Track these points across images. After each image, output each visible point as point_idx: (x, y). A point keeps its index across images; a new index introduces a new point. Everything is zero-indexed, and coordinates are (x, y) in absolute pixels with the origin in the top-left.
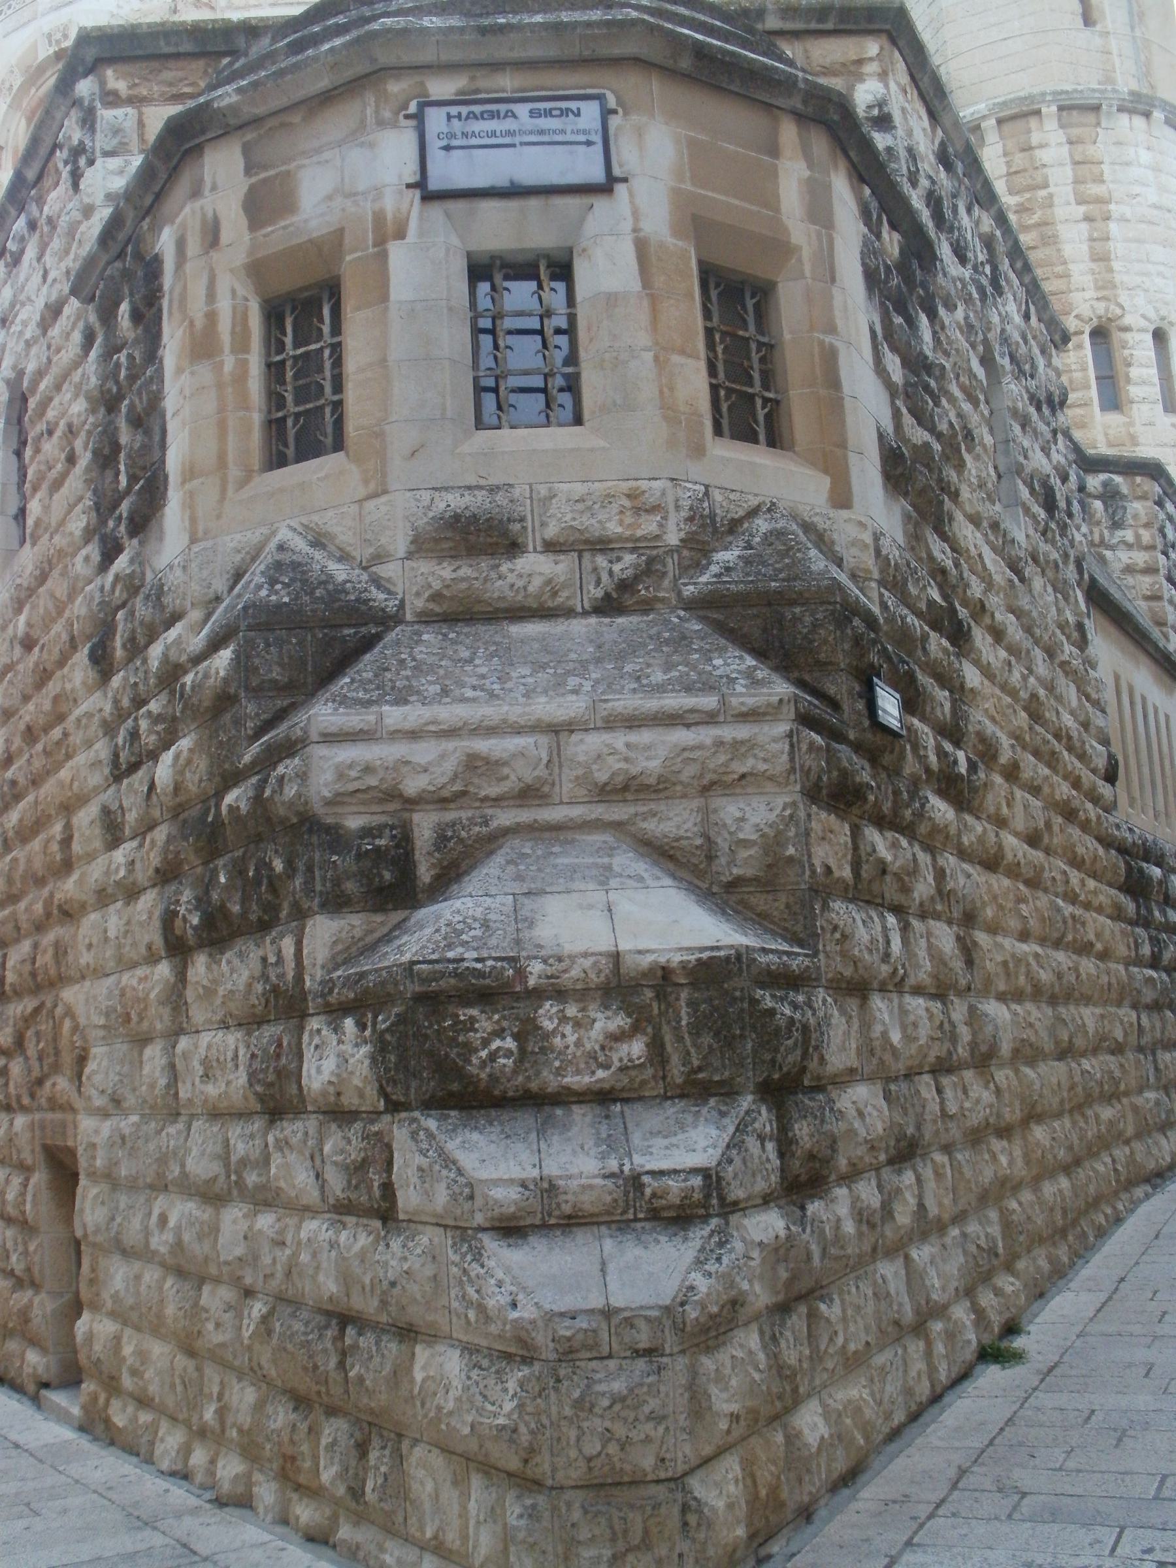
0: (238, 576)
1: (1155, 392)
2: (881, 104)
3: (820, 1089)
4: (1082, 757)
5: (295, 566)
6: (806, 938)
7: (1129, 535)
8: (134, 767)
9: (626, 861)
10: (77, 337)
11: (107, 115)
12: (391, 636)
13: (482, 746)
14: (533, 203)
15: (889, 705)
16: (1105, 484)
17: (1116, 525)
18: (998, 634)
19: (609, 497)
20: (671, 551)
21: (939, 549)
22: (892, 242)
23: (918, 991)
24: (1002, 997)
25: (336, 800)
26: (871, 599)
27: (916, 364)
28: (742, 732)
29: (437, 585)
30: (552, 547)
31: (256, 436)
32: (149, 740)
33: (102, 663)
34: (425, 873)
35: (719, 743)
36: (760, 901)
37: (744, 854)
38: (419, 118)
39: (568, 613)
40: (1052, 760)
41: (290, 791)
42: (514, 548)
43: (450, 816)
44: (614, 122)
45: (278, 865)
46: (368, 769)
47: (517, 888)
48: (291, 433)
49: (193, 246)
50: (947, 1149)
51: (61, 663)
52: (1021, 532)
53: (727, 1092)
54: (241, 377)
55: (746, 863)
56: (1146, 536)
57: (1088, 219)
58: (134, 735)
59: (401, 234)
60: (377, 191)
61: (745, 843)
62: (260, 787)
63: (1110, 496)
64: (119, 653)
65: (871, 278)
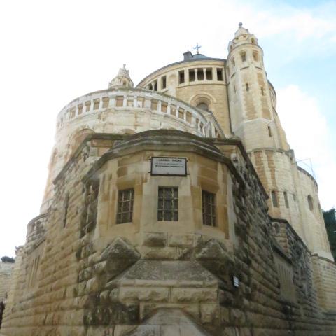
0: (108, 245)
1: (284, 204)
2: (236, 158)
4: (273, 283)
5: (120, 245)
7: (280, 234)
8: (82, 281)
9: (183, 318)
10: (81, 190)
11: (92, 149)
12: (138, 262)
13: (156, 290)
14: (172, 177)
15: (236, 281)
16: (276, 224)
17: (278, 232)
18: (256, 261)
19: (182, 237)
20: (193, 248)
21: (245, 246)
22: (238, 185)
25: (125, 299)
26: (233, 258)
27: (242, 208)
29: (148, 252)
30: (171, 246)
31: (115, 216)
32: (86, 275)
33: (78, 257)
34: (142, 316)
35: (203, 292)
37: (208, 317)
38: (152, 160)
39: (173, 260)
40: (267, 286)
41: (115, 296)
42: (163, 245)
43: (147, 304)
44: (188, 163)
45: (111, 311)
46: (132, 293)
47: (161, 323)
48: (122, 217)
49: (107, 178)
51: (70, 254)
52: (260, 238)
54: (113, 205)
55: (207, 319)
56: (284, 234)
57: (271, 171)
58: (83, 274)
59: (146, 181)
60: (142, 173)
61: (208, 315)
62: (109, 293)
63: (276, 226)
64: (82, 256)
65: (234, 193)
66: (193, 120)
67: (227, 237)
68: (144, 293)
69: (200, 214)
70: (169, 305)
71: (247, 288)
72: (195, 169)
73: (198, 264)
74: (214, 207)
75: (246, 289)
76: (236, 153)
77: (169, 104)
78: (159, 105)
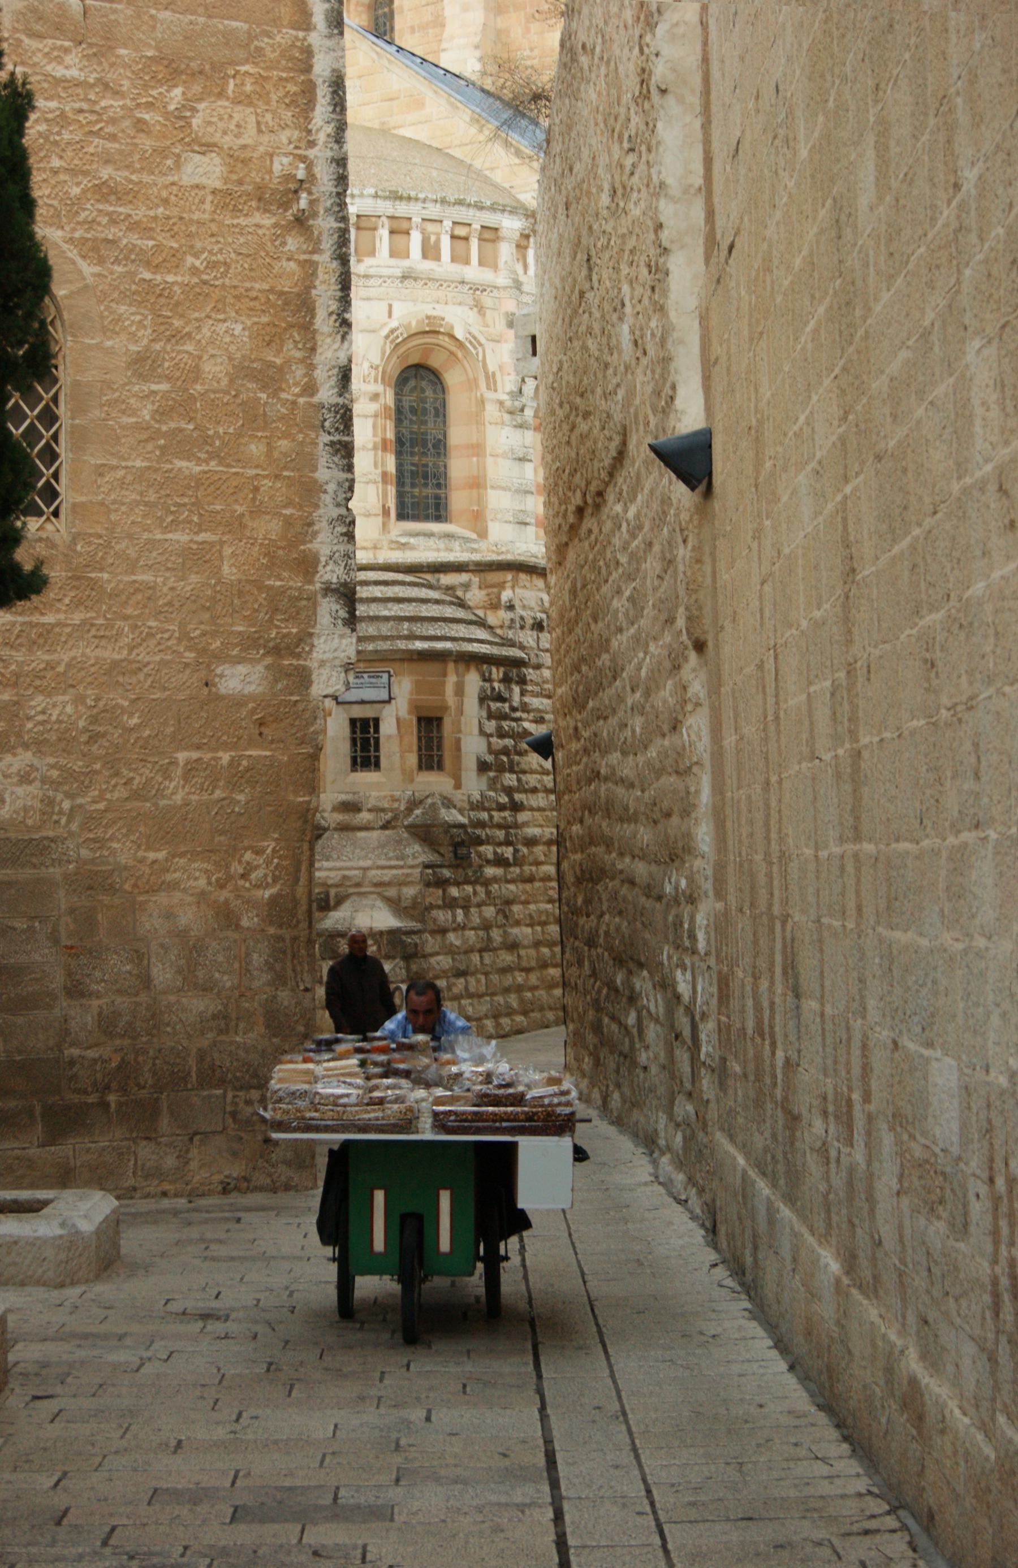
3: (424, 956)
6: (423, 921)
9: (379, 903)
12: (327, 834)
13: (347, 873)
21: (510, 779)
22: (497, 673)
23: (472, 929)
24: (531, 925)
28: (409, 871)
30: (370, 810)
34: (332, 903)
36: (411, 912)
39: (373, 829)
42: (359, 810)
50: (486, 974)
53: (394, 958)
65: (482, 700)
66: (506, 251)
67: (458, 786)
68: (334, 877)
69: (413, 759)
70: (363, 890)
71: (499, 850)
72: (404, 688)
73: (406, 835)
74: (440, 739)
75: (495, 853)
76: (513, 587)
77: (416, 220)
78: (384, 233)
